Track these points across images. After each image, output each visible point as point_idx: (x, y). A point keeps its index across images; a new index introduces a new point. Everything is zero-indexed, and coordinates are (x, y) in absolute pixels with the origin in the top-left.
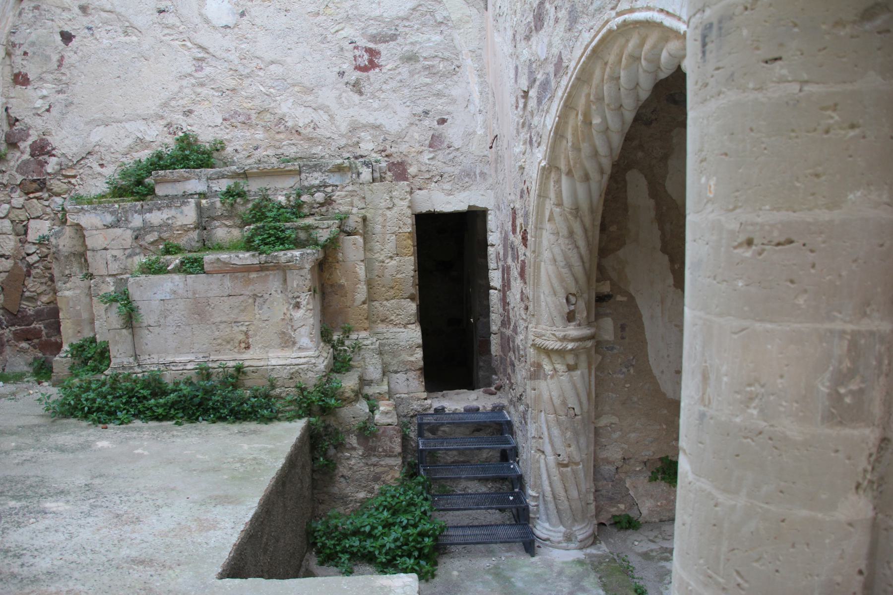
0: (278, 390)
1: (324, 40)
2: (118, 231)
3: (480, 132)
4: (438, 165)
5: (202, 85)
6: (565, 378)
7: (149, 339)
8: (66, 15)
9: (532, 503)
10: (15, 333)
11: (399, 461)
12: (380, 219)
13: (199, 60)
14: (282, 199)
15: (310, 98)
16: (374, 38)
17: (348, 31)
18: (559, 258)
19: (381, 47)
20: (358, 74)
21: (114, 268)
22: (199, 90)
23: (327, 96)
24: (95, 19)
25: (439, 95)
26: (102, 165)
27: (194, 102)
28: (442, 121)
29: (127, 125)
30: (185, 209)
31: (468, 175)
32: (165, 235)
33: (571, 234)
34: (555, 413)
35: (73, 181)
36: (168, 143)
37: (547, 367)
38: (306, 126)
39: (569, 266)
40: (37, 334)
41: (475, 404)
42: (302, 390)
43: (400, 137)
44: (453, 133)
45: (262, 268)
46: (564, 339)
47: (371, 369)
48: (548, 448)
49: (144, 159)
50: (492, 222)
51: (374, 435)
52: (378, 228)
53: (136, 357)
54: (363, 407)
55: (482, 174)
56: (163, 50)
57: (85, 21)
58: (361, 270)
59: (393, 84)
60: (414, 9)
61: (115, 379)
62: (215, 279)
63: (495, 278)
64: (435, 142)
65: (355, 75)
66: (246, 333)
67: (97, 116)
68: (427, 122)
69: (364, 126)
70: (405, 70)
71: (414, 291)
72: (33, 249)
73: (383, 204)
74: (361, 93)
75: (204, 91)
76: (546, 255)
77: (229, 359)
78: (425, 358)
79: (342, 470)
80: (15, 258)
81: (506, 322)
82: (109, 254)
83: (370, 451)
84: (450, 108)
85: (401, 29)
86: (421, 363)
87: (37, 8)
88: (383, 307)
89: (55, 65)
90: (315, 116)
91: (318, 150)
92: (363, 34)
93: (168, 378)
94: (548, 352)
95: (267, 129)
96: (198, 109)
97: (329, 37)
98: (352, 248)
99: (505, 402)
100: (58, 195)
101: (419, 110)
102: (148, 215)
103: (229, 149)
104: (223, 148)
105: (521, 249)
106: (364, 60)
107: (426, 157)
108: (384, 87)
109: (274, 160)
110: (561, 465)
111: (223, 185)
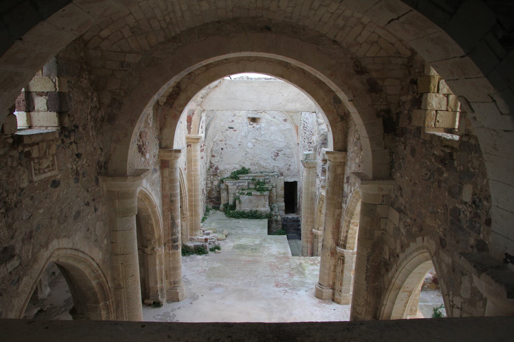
1: (269, 151)
2: (234, 186)
3: (297, 168)
5: (246, 158)
7: (242, 205)
10: (209, 201)
11: (281, 226)
12: (278, 184)
13: (246, 154)
14: (261, 181)
16: (278, 151)
21: (233, 192)
23: (269, 161)
24: (227, 146)
25: (289, 161)
28: (290, 166)
30: (246, 183)
32: (242, 187)
36: (239, 168)
38: (265, 166)
40: (213, 201)
41: (294, 217)
42: (267, 214)
43: (282, 168)
45: (261, 195)
47: (276, 210)
51: (277, 221)
52: (278, 186)
54: (276, 217)
55: (297, 175)
57: (226, 146)
58: (275, 194)
59: (281, 159)
61: (237, 212)
64: (288, 169)
68: (287, 166)
70: (283, 156)
71: (284, 197)
72: (214, 186)
73: (279, 182)
75: (247, 159)
77: (254, 209)
78: (285, 208)
79: (272, 227)
80: (211, 187)
81: (300, 202)
82: (232, 190)
83: (277, 224)
84: (291, 163)
88: (279, 199)
91: (267, 170)
93: (245, 212)
95: (258, 166)
96: (246, 162)
98: (274, 190)
99: (299, 216)
101: (286, 164)
103: (251, 170)
104: (250, 169)
111: (251, 178)
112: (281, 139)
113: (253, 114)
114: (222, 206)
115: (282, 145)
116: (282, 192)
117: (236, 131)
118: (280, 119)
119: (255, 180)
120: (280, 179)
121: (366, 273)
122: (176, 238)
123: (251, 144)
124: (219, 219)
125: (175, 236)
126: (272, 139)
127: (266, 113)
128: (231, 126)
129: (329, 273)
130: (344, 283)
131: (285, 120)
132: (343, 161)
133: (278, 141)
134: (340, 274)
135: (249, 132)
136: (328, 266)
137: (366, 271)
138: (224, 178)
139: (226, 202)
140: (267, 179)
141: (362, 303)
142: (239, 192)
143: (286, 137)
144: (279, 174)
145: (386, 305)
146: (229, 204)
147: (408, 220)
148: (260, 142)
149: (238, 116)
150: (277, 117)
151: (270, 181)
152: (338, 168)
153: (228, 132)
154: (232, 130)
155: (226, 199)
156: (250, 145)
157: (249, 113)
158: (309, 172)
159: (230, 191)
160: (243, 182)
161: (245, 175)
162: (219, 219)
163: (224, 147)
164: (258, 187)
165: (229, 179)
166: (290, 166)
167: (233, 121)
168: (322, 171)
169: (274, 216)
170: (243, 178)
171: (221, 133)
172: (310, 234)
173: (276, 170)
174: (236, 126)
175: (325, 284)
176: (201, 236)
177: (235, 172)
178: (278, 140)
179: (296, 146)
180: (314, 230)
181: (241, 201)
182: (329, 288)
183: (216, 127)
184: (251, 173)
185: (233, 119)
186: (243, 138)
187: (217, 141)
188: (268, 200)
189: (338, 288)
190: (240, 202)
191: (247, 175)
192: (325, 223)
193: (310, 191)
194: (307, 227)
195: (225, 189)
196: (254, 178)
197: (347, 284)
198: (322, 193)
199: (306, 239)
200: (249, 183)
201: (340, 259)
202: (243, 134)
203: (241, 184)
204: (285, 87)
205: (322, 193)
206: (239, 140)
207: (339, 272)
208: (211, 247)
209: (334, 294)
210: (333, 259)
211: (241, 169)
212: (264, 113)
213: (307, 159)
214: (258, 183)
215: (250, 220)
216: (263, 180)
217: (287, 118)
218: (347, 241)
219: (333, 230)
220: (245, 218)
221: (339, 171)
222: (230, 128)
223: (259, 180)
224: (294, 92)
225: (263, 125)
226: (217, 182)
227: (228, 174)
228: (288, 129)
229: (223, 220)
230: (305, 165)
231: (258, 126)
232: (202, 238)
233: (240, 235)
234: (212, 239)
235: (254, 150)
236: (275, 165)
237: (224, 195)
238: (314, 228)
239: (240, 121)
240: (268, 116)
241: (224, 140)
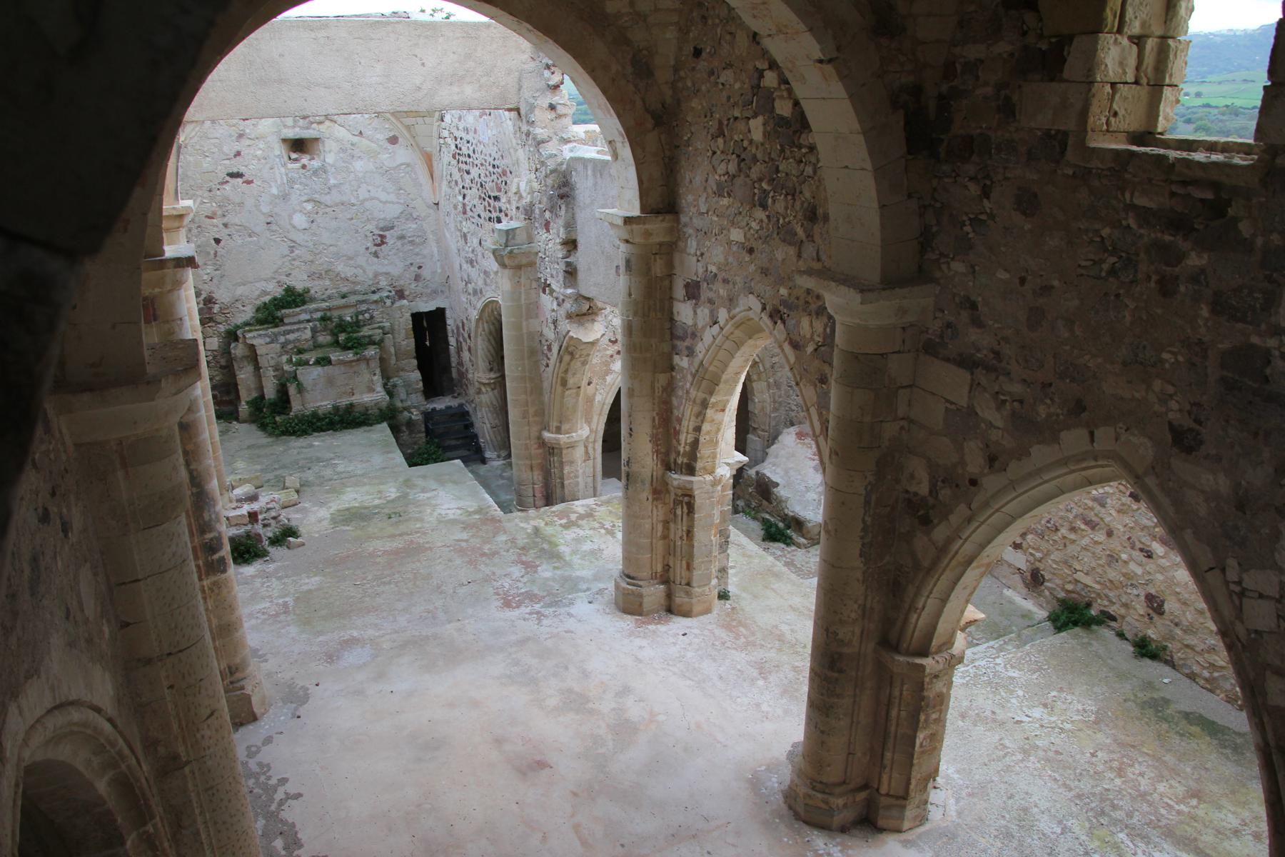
0: (370, 412)
1: (357, 232)
3: (439, 271)
4: (419, 289)
5: (294, 260)
6: (491, 394)
7: (308, 396)
8: (215, 229)
9: (482, 445)
11: (424, 435)
12: (397, 323)
14: (349, 319)
15: (352, 262)
16: (382, 229)
17: (371, 227)
18: (486, 350)
19: (386, 233)
20: (376, 248)
21: (272, 363)
22: (293, 262)
23: (361, 260)
24: (231, 230)
25: (417, 254)
26: (244, 306)
27: (291, 269)
28: (420, 267)
29: (256, 284)
31: (435, 292)
33: (489, 340)
34: (488, 407)
35: (228, 315)
36: (278, 292)
37: (483, 389)
38: (351, 276)
39: (489, 351)
41: (449, 404)
44: (426, 273)
45: (358, 360)
46: (490, 379)
48: (487, 422)
49: (267, 302)
50: (448, 314)
53: (303, 405)
54: (406, 413)
55: (442, 291)
56: (272, 243)
57: (227, 231)
58: (392, 350)
59: (394, 251)
60: (402, 213)
62: (336, 368)
63: (452, 341)
64: (417, 278)
65: (374, 249)
66: (352, 389)
67: (239, 281)
68: (412, 268)
69: (381, 274)
70: (399, 243)
71: (415, 354)
73: (398, 316)
74: (378, 257)
75: (296, 263)
76: (480, 347)
77: (344, 401)
78: (424, 385)
82: (269, 357)
83: (411, 432)
85: (396, 223)
86: (422, 389)
87: (199, 227)
89: (212, 256)
90: (355, 271)
91: (358, 288)
92: (377, 228)
93: (320, 412)
94: (484, 384)
95: (331, 280)
96: (294, 273)
97: (360, 230)
100: (220, 323)
101: (408, 263)
102: (287, 336)
103: (312, 292)
105: (468, 341)
106: (379, 241)
107: (413, 286)
108: (390, 253)
109: (336, 295)
110: (492, 428)
111: (319, 315)
112: (388, 193)
113: (297, 129)
114: (244, 408)
115: (392, 211)
116: (409, 344)
117: (251, 182)
118: (378, 136)
119: (330, 319)
120: (400, 308)
121: (862, 538)
122: (215, 538)
123: (304, 218)
124: (249, 447)
125: (210, 532)
126: (361, 198)
127: (335, 122)
128: (235, 170)
129: (652, 543)
130: (697, 561)
131: (393, 140)
132: (667, 239)
133: (381, 202)
134: (684, 542)
135: (291, 182)
136: (648, 527)
137: (862, 534)
138: (238, 327)
139: (255, 395)
140: (362, 313)
141: (853, 615)
142: (290, 361)
143: (401, 189)
144: (393, 293)
145: (924, 607)
146: (267, 397)
147: (1017, 388)
148: (328, 210)
149: (253, 136)
150: (367, 132)
151: (372, 317)
152: (655, 260)
153: (227, 187)
154: (240, 180)
155: (253, 386)
156: (300, 220)
157: (285, 126)
158: (517, 279)
159: (263, 362)
160: (298, 330)
161: (298, 310)
162: (249, 447)
163: (222, 234)
164: (342, 337)
165: (253, 328)
166: (420, 267)
167: (238, 154)
168: (566, 272)
169: (402, 412)
170: (295, 319)
171: (206, 194)
172: (536, 446)
173: (383, 283)
174: (251, 167)
175: (645, 573)
176: (234, 509)
177: (265, 304)
178: (378, 199)
179: (431, 211)
180: (547, 435)
181: (302, 385)
182: (655, 581)
183: (187, 176)
184: (312, 300)
185: (239, 149)
186: (277, 201)
187: (197, 219)
188: (378, 371)
189: (681, 578)
190: (301, 389)
191: (303, 308)
192: (630, 416)
193: (525, 331)
194: (527, 428)
195: (248, 357)
196: (325, 314)
197: (703, 562)
198: (571, 334)
199: (528, 462)
200: (314, 330)
201: (681, 502)
202: (275, 191)
203: (291, 337)
204: (426, 37)
205: (571, 334)
206: (265, 209)
207: (681, 538)
208: (270, 535)
209: (669, 596)
210: (660, 506)
211: (283, 293)
212: (328, 123)
213: (509, 244)
214: (342, 327)
215: (338, 434)
216: (352, 317)
217: (397, 134)
218: (698, 455)
219: (655, 431)
220: (324, 431)
221: (658, 268)
222: (232, 175)
223: (340, 318)
224: (454, 53)
225: (330, 159)
226: (216, 339)
227: (247, 314)
228: (402, 164)
229: (263, 446)
230: (506, 261)
231: (316, 163)
232: (238, 512)
233: (333, 482)
234: (268, 509)
235: (314, 234)
236: (380, 271)
237: (244, 375)
238: (546, 427)
239: (259, 153)
240: (341, 133)
241: (219, 213)
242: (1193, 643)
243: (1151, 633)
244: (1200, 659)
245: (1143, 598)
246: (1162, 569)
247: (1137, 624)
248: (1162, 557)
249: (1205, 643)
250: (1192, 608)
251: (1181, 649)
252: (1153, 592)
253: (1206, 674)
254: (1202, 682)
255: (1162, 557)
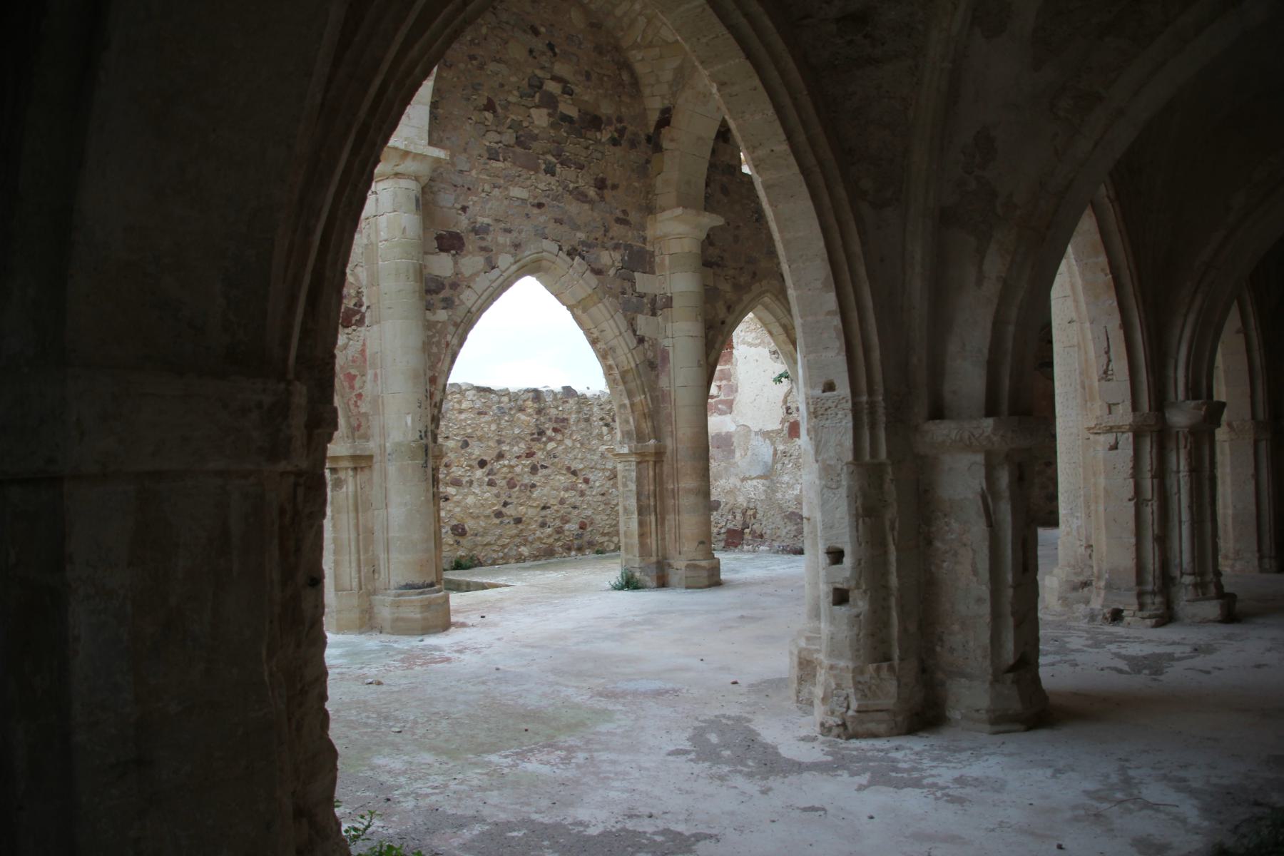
147: (731, 272)
242: (489, 540)
243: (461, 553)
244: (495, 548)
245: (450, 532)
246: (458, 503)
247: (450, 553)
248: (455, 495)
249: (495, 535)
250: (482, 518)
251: (482, 549)
252: (455, 522)
253: (501, 554)
254: (501, 561)
255: (455, 495)
